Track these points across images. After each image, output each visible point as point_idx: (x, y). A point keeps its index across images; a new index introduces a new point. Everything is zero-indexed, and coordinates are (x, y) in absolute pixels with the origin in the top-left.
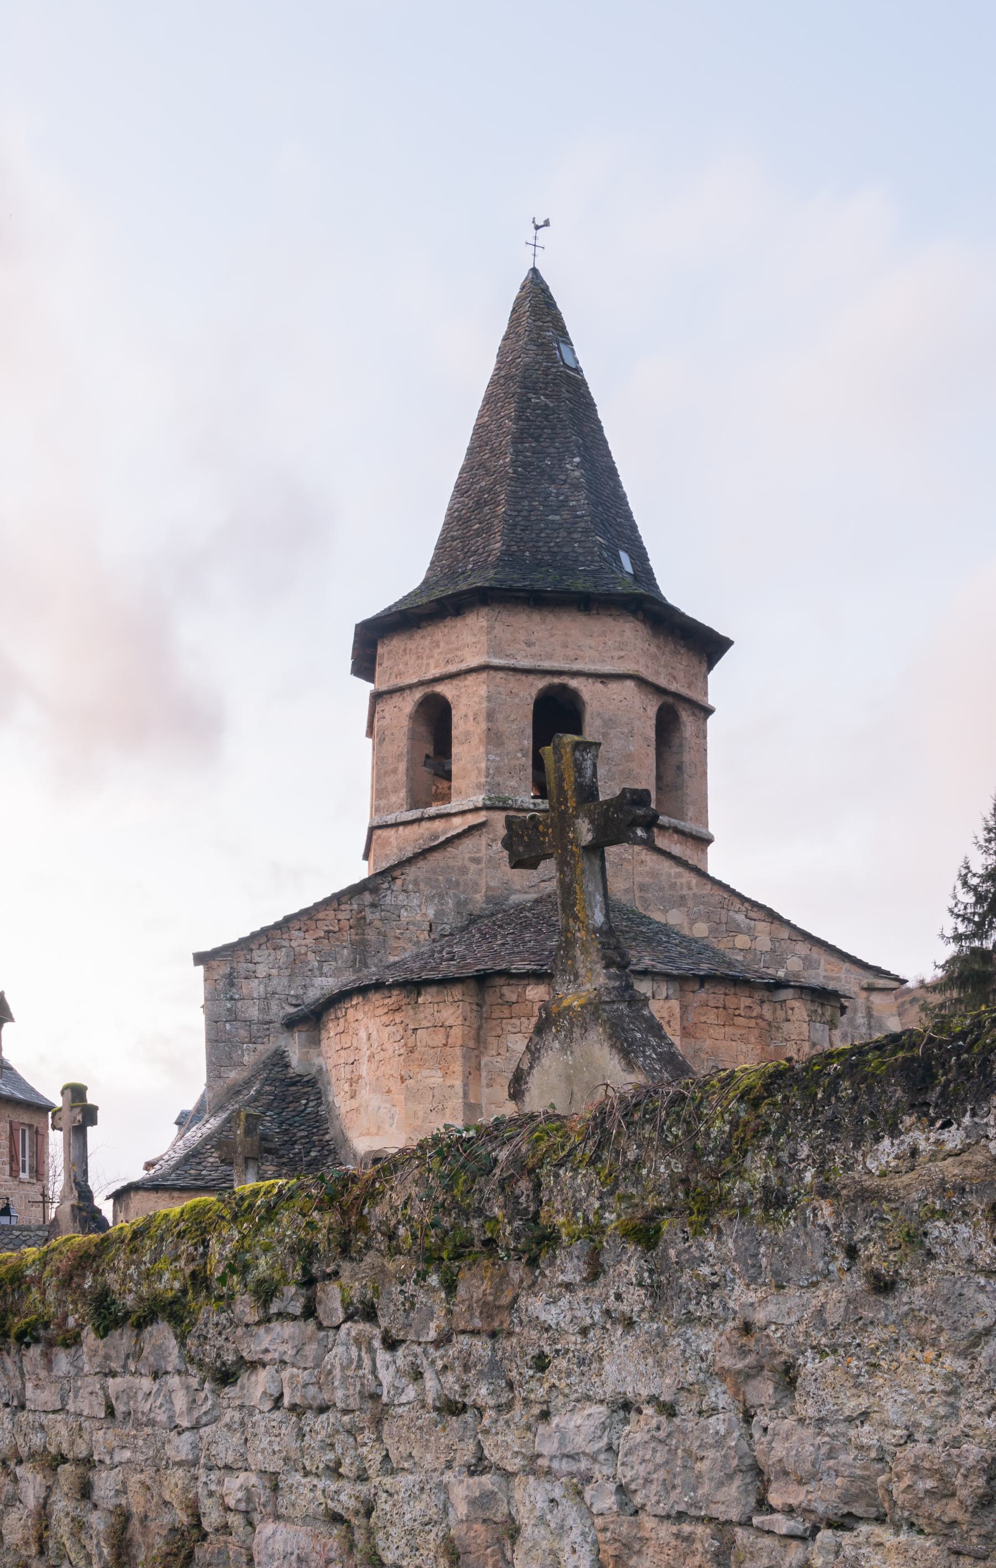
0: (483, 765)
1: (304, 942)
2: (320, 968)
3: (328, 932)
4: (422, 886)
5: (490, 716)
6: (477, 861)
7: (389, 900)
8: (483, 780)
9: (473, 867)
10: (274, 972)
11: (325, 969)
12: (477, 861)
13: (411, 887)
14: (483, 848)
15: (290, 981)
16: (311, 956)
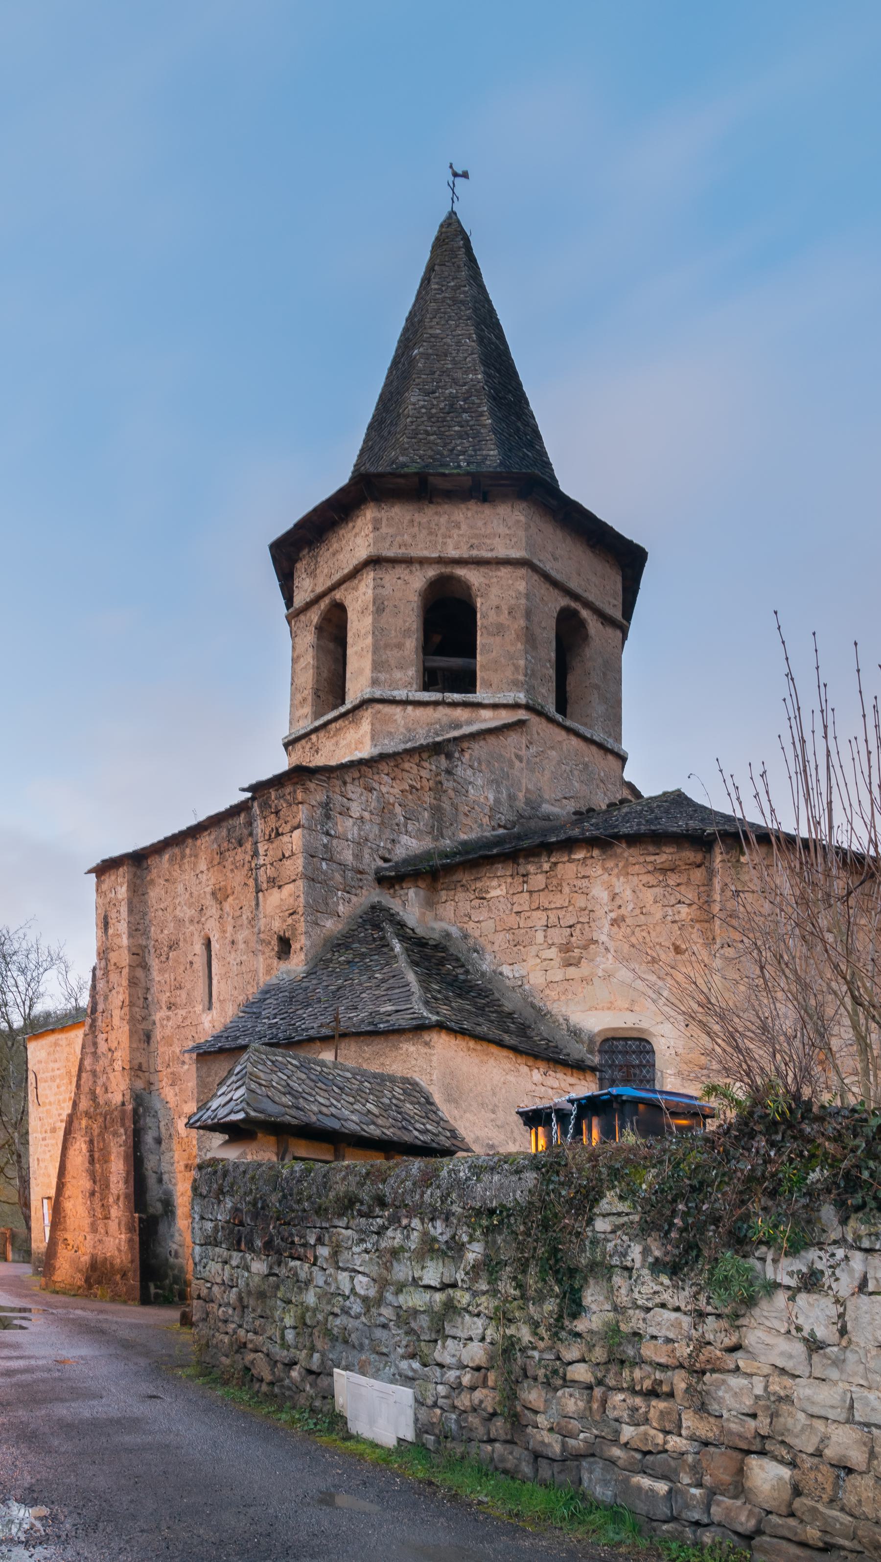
0: (522, 663)
1: (392, 790)
2: (406, 826)
3: (412, 786)
4: (483, 767)
5: (528, 614)
6: (519, 758)
7: (459, 771)
8: (521, 678)
9: (517, 763)
10: (366, 815)
11: (410, 827)
12: (519, 758)
13: (476, 764)
14: (524, 746)
15: (380, 830)
16: (398, 809)
